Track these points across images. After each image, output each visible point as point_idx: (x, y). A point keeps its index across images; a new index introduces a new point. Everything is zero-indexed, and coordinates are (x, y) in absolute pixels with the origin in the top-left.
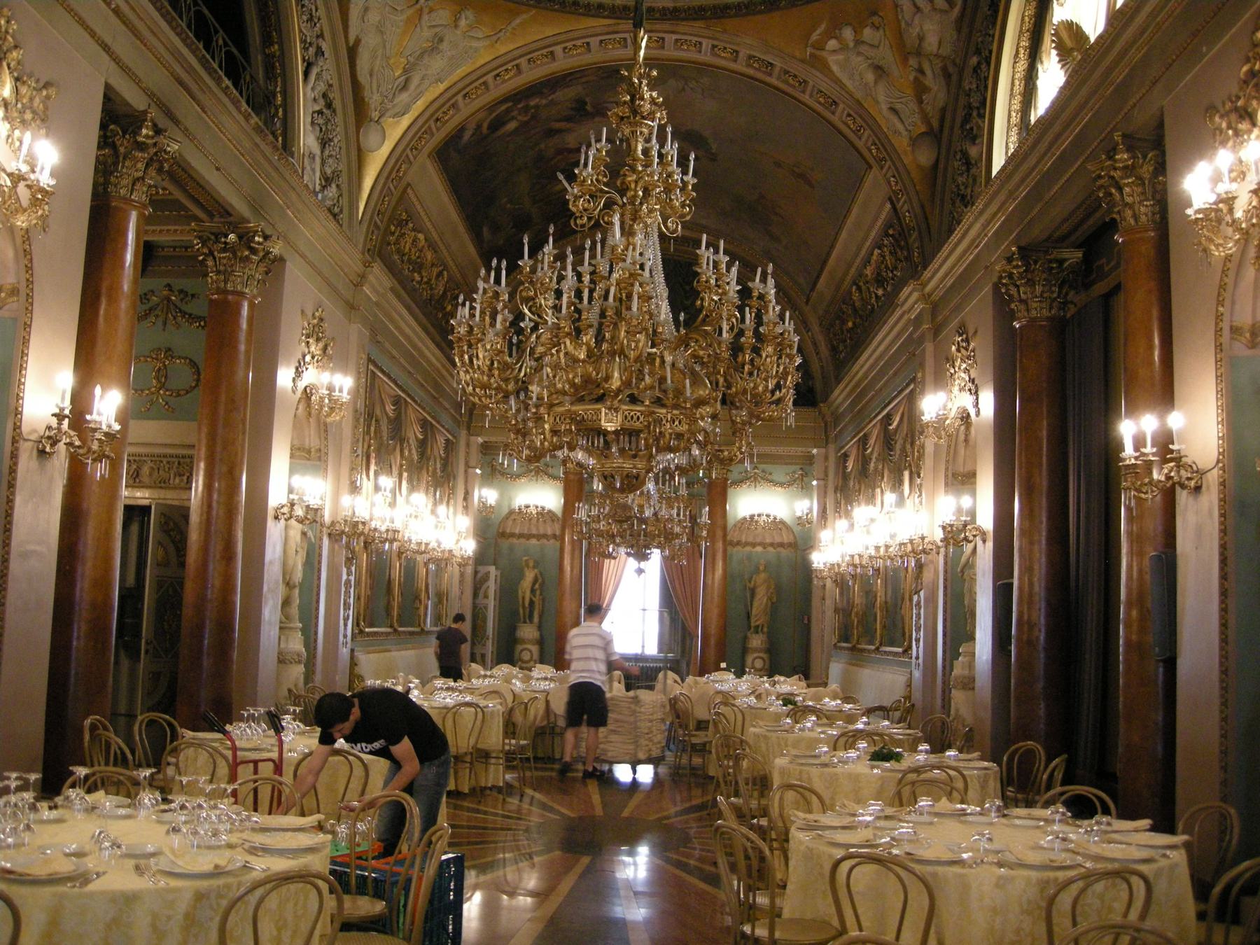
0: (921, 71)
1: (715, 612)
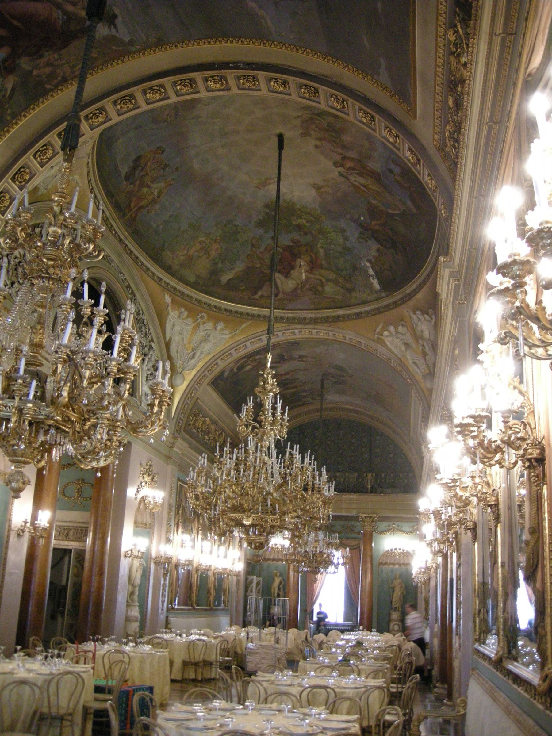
0: (423, 346)
1: (367, 600)
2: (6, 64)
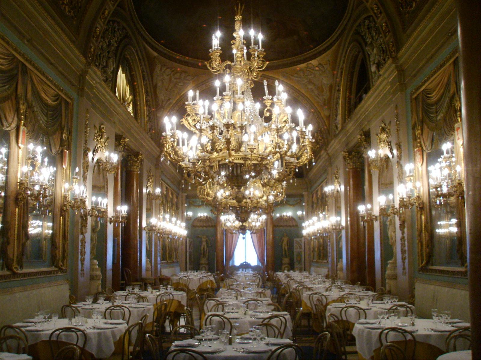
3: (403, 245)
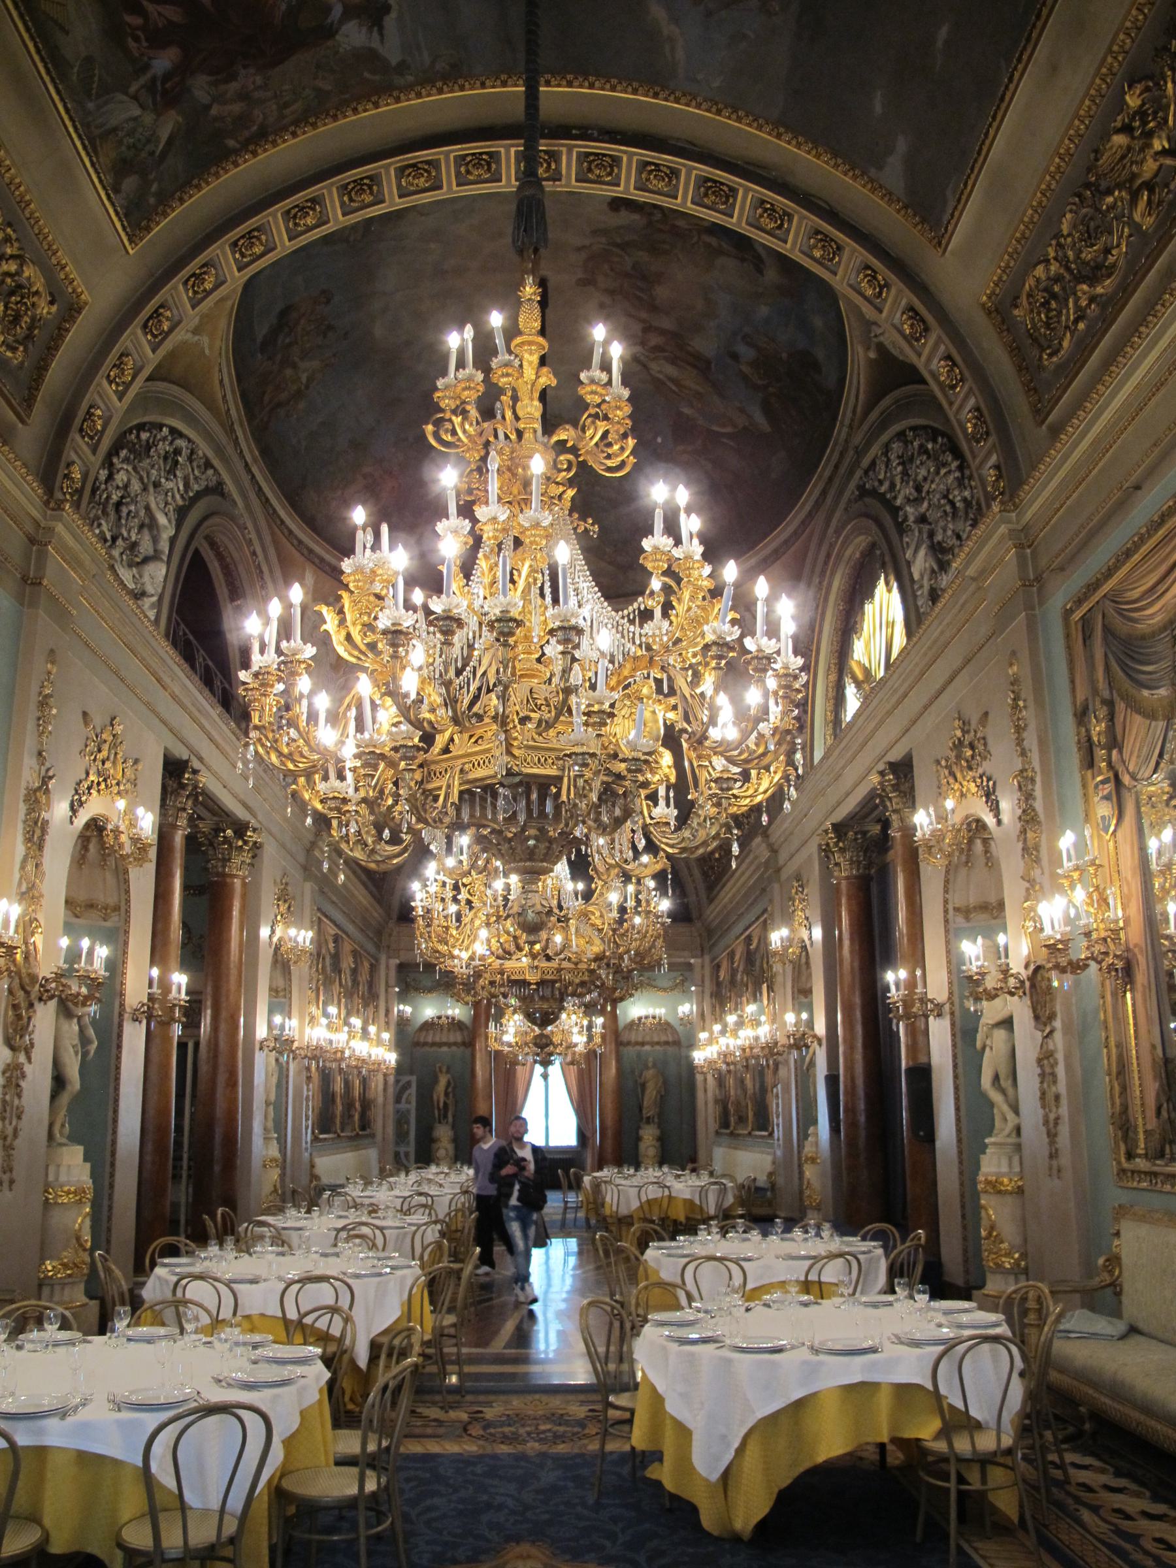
1: (609, 1106)
2: (168, 85)
3: (1047, 1076)
